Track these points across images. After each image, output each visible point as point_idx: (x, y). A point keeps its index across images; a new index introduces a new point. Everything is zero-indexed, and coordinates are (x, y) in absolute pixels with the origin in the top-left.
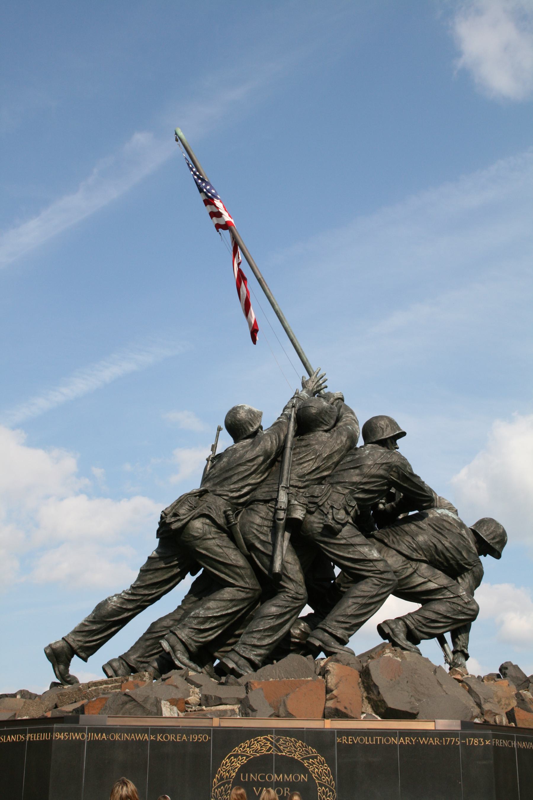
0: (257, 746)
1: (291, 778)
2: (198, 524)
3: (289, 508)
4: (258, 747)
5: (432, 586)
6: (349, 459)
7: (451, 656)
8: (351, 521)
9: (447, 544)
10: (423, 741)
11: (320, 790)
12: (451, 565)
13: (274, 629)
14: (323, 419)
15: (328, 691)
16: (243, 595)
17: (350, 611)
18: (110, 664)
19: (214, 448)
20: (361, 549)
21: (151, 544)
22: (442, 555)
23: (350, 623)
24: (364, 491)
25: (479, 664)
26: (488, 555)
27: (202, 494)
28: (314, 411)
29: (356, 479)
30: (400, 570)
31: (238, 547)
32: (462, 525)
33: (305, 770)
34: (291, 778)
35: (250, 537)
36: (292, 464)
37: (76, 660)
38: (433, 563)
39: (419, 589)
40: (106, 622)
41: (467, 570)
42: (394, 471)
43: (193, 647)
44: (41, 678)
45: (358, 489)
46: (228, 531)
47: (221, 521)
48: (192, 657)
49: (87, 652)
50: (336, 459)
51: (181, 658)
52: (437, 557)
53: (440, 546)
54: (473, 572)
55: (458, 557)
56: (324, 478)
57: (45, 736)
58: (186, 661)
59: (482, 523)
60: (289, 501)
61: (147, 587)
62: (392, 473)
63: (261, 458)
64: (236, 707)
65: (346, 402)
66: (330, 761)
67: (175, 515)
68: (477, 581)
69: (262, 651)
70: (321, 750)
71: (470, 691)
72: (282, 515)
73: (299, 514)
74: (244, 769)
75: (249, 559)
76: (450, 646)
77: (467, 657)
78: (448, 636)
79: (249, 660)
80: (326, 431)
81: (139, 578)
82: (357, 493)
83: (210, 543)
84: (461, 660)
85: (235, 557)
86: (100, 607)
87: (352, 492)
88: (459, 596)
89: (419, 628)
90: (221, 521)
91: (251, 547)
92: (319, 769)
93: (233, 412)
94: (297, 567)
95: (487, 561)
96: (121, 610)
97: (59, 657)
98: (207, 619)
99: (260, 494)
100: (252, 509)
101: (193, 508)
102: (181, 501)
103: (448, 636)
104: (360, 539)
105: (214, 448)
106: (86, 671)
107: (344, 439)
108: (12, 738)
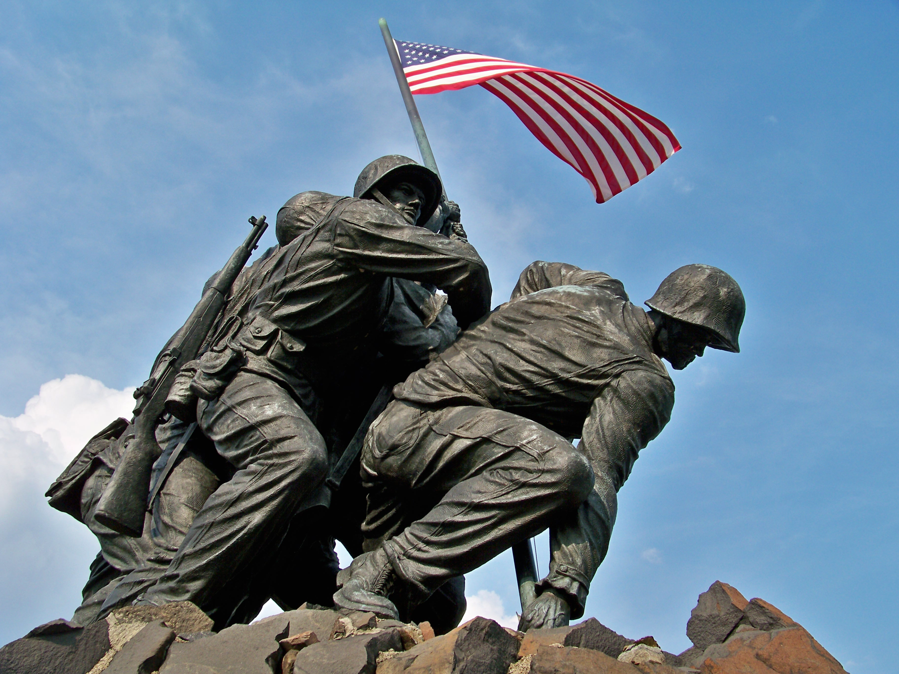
12: (541, 389)
14: (302, 221)
20: (245, 411)
22: (508, 375)
23: (177, 576)
26: (707, 349)
30: (402, 438)
41: (598, 391)
42: (340, 235)
45: (276, 300)
52: (500, 383)
54: (615, 390)
55: (556, 366)
62: (338, 240)
82: (277, 309)
88: (518, 449)
89: (415, 553)
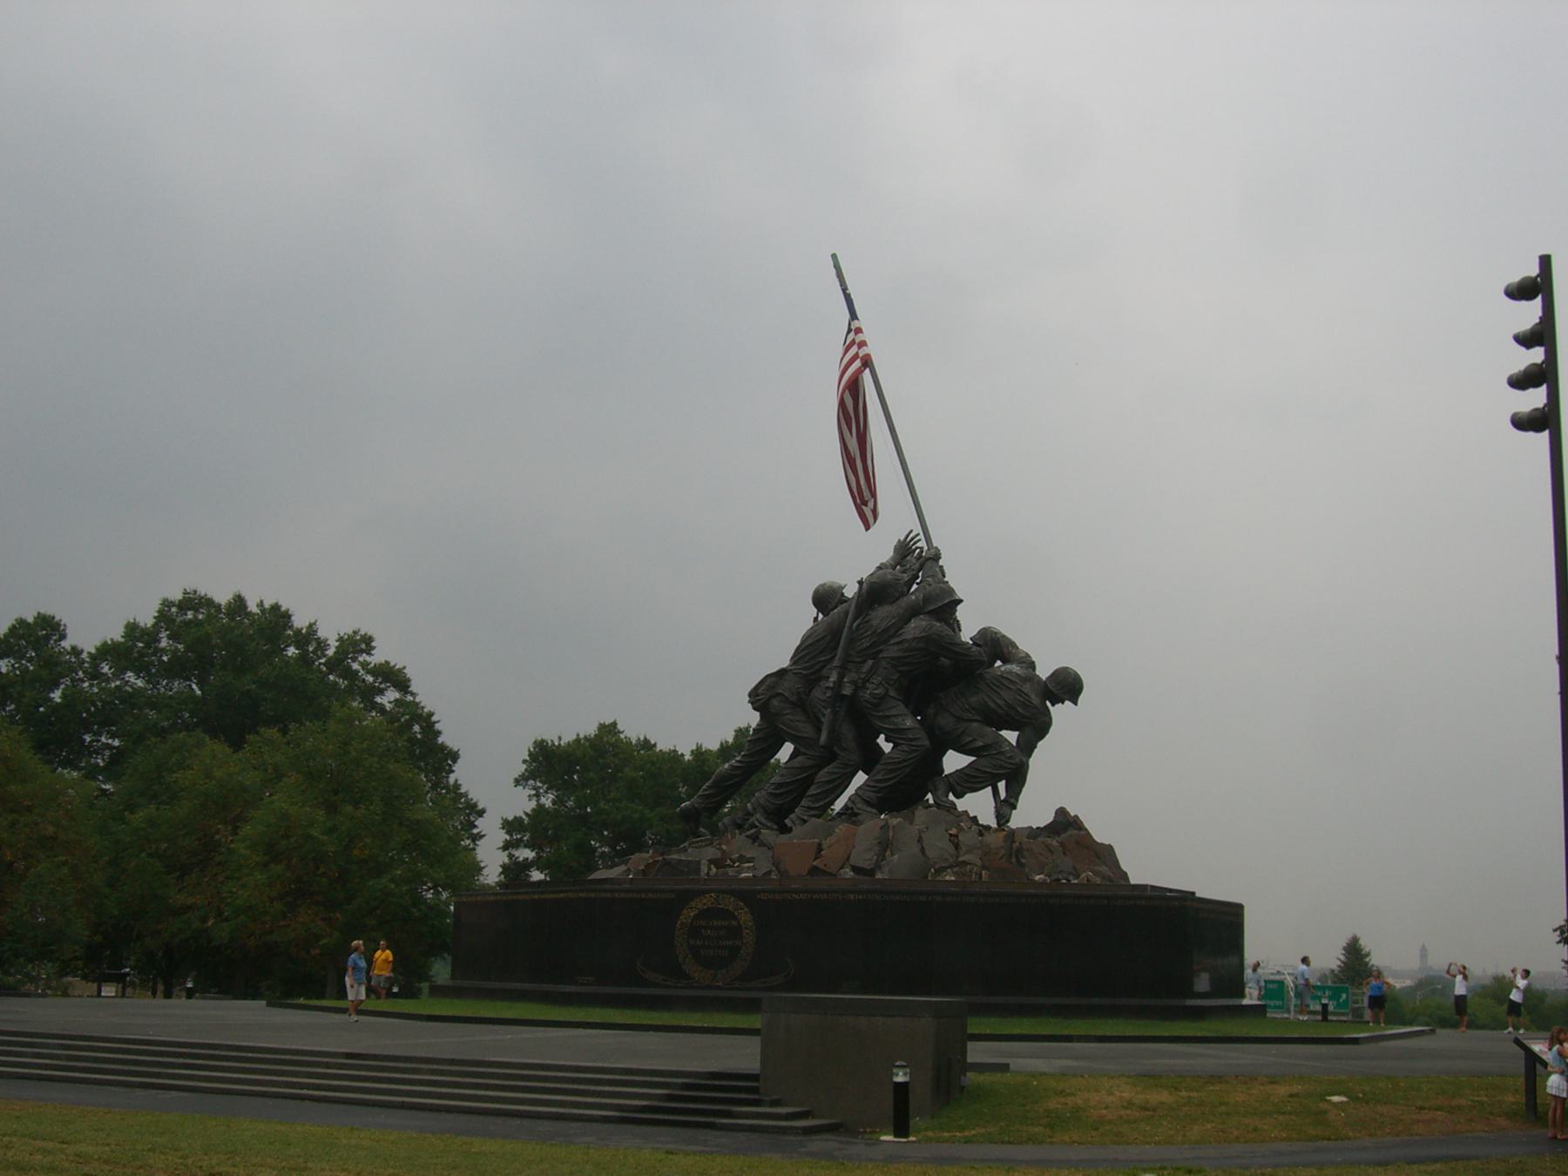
1: (725, 923)
2: (775, 702)
8: (892, 693)
15: (820, 849)
16: (810, 763)
17: (879, 777)
25: (1032, 811)
33: (735, 918)
34: (725, 923)
36: (851, 641)
46: (801, 704)
47: (794, 698)
53: (992, 705)
60: (841, 676)
71: (957, 846)
73: (847, 691)
76: (1003, 795)
77: (1014, 807)
90: (794, 698)
92: (745, 917)
95: (1060, 712)
98: (780, 785)
101: (771, 687)
103: (1002, 785)
104: (902, 708)
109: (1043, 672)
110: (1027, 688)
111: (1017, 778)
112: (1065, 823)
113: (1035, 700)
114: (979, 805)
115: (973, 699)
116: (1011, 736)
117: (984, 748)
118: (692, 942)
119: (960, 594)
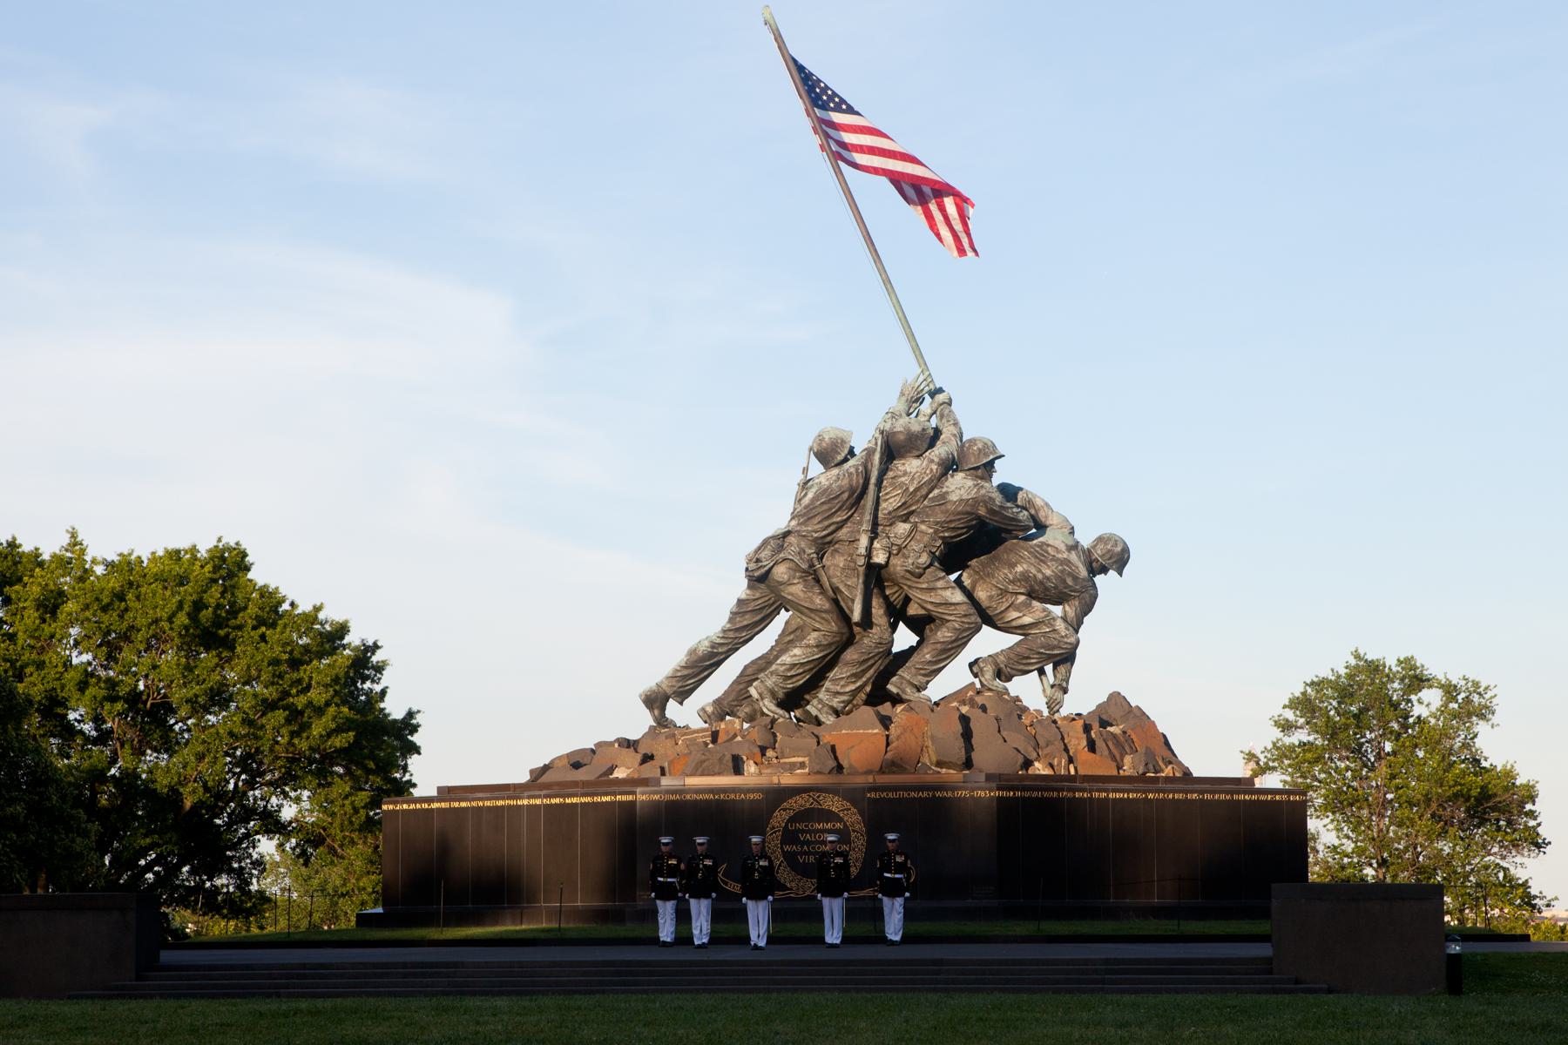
0: (801, 801)
1: (829, 826)
3: (870, 549)
4: (800, 802)
5: (1027, 620)
6: (936, 492)
7: (1049, 691)
9: (1048, 572)
10: (938, 794)
11: (853, 835)
13: (857, 676)
18: (703, 709)
19: (805, 470)
21: (739, 587)
24: (949, 529)
25: (1082, 698)
27: (786, 534)
28: (902, 437)
29: (941, 518)
31: (823, 592)
32: (1075, 547)
33: (840, 820)
35: (834, 580)
37: (672, 705)
38: (1031, 595)
39: (1014, 624)
40: (702, 666)
43: (781, 695)
44: (638, 723)
46: (812, 575)
48: (780, 705)
49: (683, 695)
50: (924, 492)
51: (769, 706)
53: (1040, 576)
56: (912, 512)
57: (630, 798)
58: (773, 708)
59: (1100, 539)
60: (871, 543)
61: (737, 630)
63: (846, 495)
64: (806, 759)
65: (953, 407)
66: (861, 813)
67: (758, 561)
68: (1087, 608)
69: (845, 698)
70: (854, 803)
72: (861, 561)
73: (880, 558)
74: (792, 820)
75: (836, 602)
76: (1052, 680)
77: (1065, 691)
78: (1049, 668)
79: (832, 708)
80: (918, 457)
81: (731, 620)
83: (793, 589)
84: (1058, 694)
85: (819, 601)
86: (693, 652)
87: (936, 532)
91: (836, 590)
93: (820, 438)
94: (881, 612)
96: (711, 655)
97: (655, 701)
99: (843, 533)
100: (836, 551)
102: (765, 543)
103: (1049, 668)
105: (805, 470)
106: (686, 714)
107: (934, 467)
108: (605, 799)
109: (1085, 539)
110: (1073, 557)
111: (1066, 658)
112: (1116, 711)
113: (1083, 572)
114: (1029, 690)
115: (1019, 569)
116: (1057, 610)
117: (1031, 625)
118: (787, 848)
119: (1001, 450)
